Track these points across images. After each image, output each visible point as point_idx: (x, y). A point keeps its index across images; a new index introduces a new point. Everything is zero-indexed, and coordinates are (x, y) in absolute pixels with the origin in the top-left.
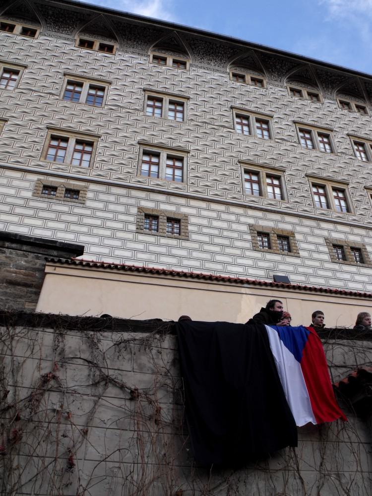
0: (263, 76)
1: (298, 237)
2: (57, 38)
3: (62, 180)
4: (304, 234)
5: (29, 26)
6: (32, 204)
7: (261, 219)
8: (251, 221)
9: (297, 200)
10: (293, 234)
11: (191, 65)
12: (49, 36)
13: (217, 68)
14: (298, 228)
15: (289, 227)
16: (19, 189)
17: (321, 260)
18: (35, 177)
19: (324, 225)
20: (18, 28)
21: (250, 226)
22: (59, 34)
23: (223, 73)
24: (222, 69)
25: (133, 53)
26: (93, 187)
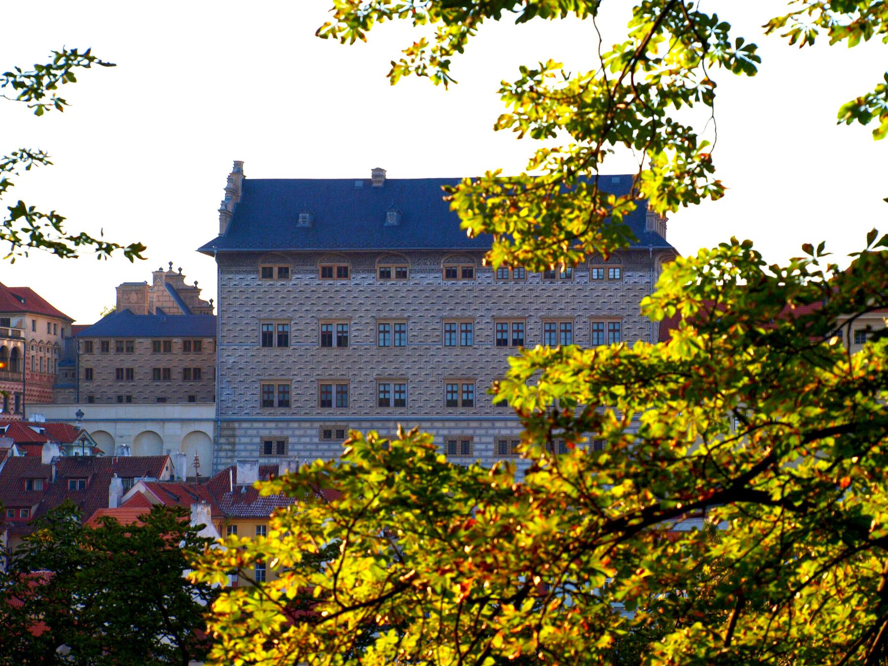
0: (473, 262)
1: (476, 439)
2: (305, 273)
3: (333, 424)
4: (480, 436)
5: (282, 265)
6: (321, 447)
7: (453, 428)
8: (446, 432)
9: (482, 404)
10: (472, 438)
11: (410, 272)
12: (299, 273)
13: (433, 267)
14: (478, 432)
15: (470, 432)
16: (311, 436)
17: (487, 457)
18: (317, 425)
19: (498, 424)
20: (275, 271)
21: (445, 437)
22: (305, 268)
23: (437, 272)
24: (436, 267)
25: (364, 271)
26: (351, 425)
